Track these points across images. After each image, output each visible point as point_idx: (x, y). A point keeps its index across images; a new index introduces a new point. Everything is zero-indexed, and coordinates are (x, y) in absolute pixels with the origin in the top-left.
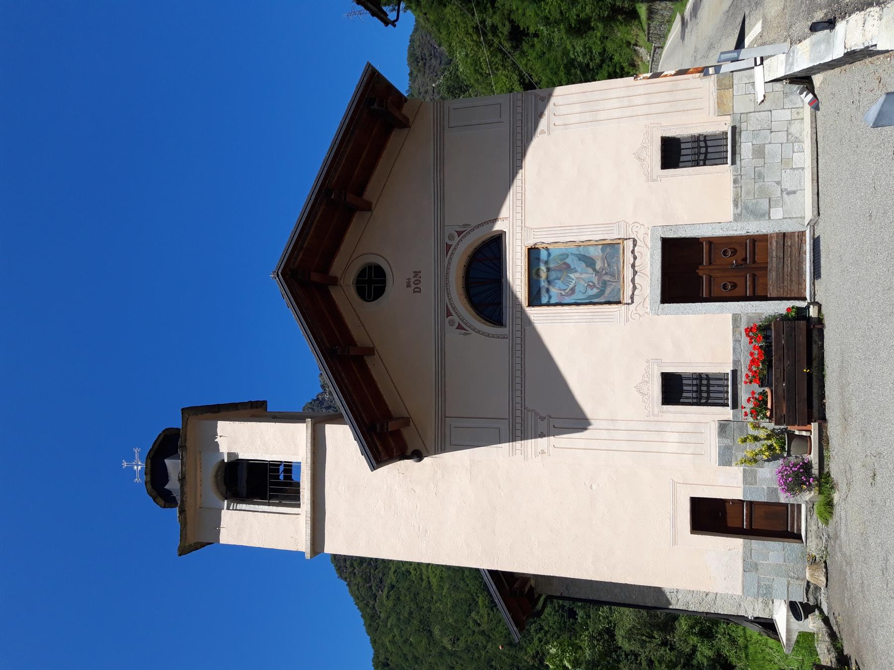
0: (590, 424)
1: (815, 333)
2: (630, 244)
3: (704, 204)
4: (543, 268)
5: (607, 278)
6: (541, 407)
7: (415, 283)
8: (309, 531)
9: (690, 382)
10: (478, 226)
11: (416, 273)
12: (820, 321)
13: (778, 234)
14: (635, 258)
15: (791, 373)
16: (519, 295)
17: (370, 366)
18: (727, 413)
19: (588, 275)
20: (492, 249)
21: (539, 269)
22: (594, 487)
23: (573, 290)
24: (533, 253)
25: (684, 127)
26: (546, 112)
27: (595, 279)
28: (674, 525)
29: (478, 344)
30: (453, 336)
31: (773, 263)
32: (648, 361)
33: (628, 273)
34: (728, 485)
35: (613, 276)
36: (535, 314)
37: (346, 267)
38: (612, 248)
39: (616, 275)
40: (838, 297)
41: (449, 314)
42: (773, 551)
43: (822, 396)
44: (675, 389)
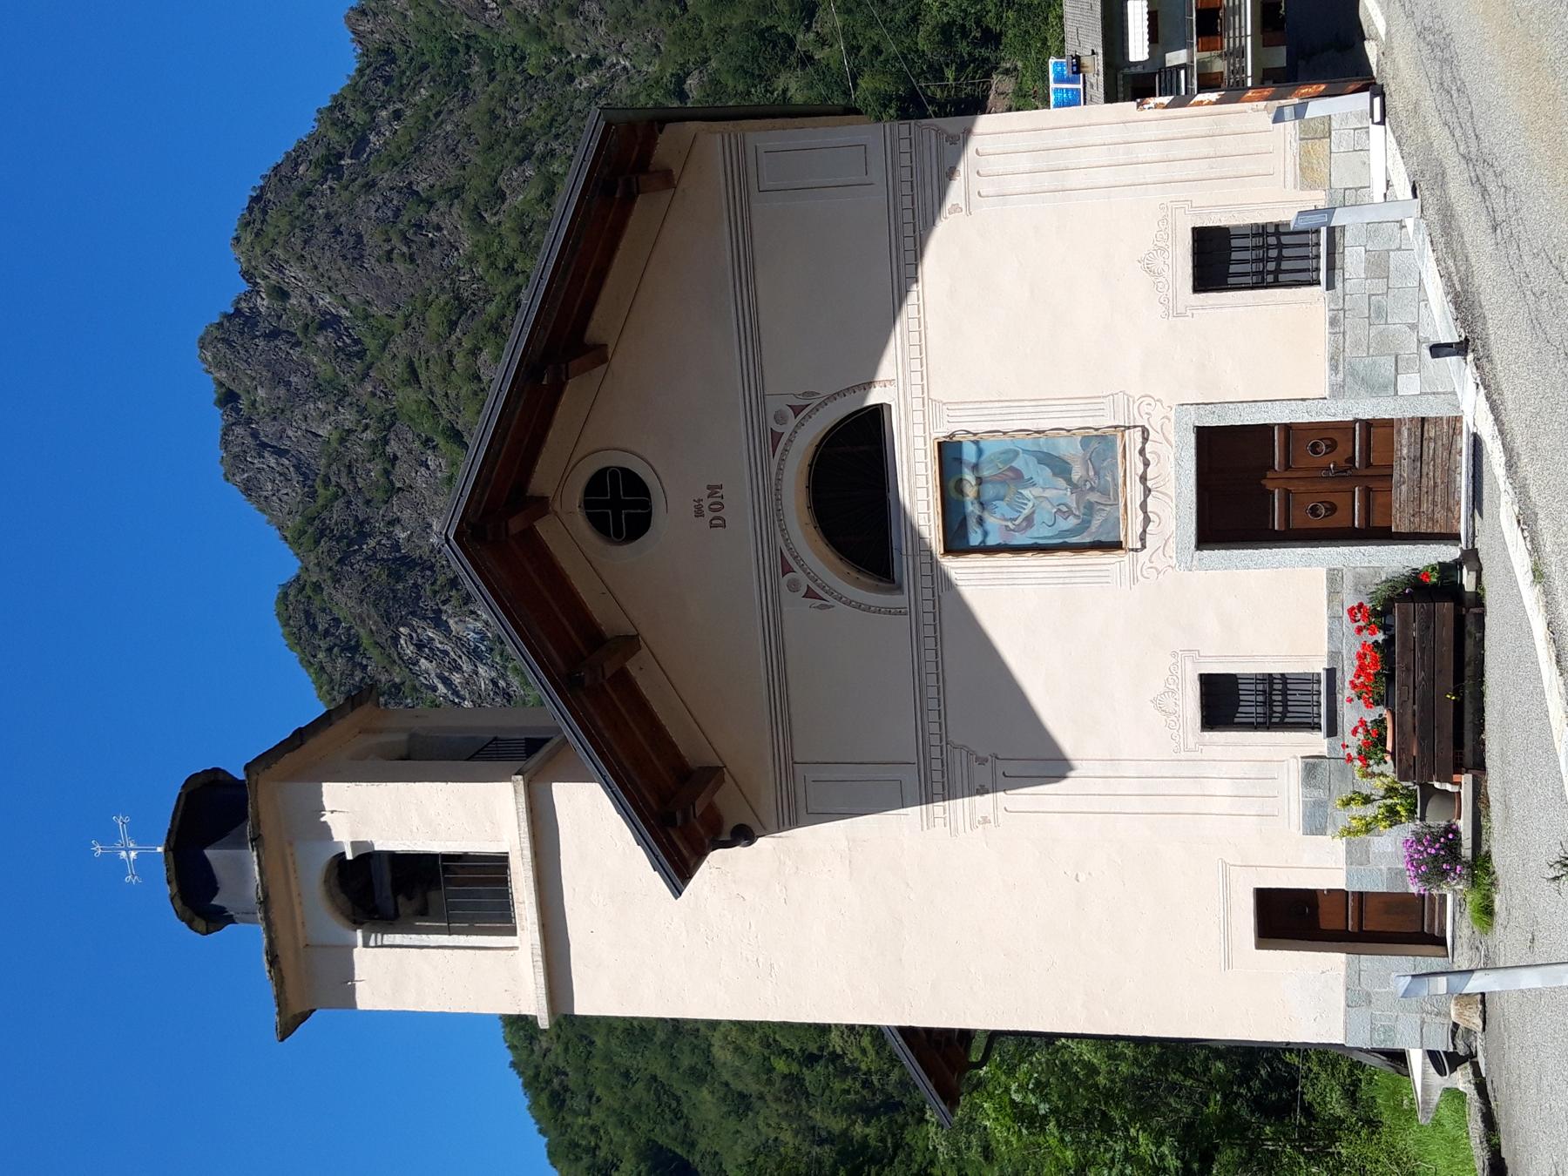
0: (1071, 769)
3: (1275, 361)
4: (969, 477)
5: (1093, 497)
6: (979, 738)
7: (712, 507)
8: (541, 980)
10: (833, 397)
11: (714, 489)
14: (1146, 464)
16: (925, 531)
18: (1316, 742)
19: (1059, 491)
20: (861, 443)
23: (1029, 520)
24: (949, 454)
26: (961, 168)
27: (1072, 500)
28: (1227, 937)
30: (796, 610)
31: (1403, 470)
32: (1174, 654)
33: (1134, 492)
34: (1321, 866)
35: (1105, 493)
36: (959, 569)
38: (1100, 444)
41: (787, 569)
42: (1392, 971)
44: (1223, 702)
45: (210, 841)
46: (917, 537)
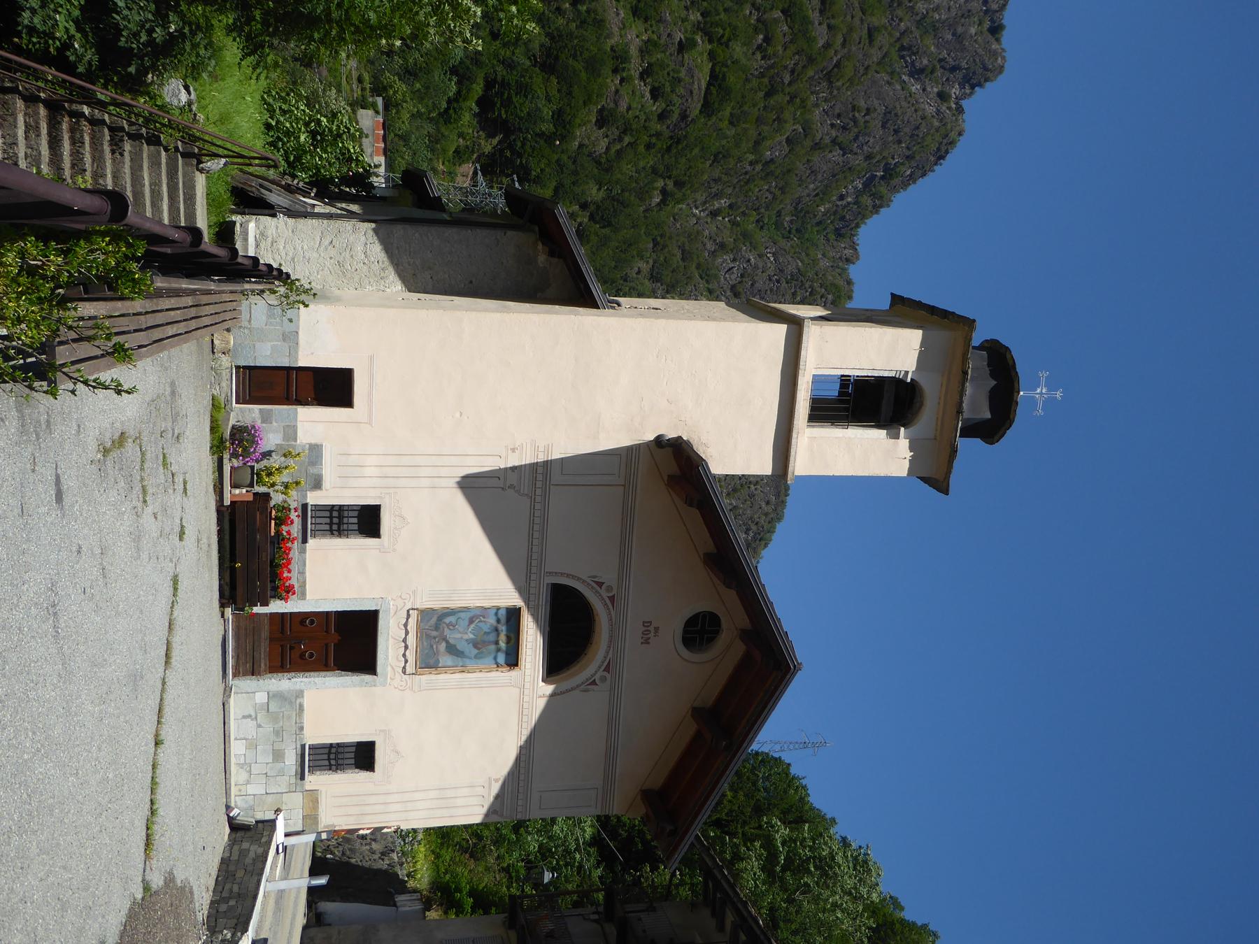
0: (458, 483)
1: (227, 593)
2: (410, 669)
3: (331, 705)
4: (503, 645)
5: (434, 633)
6: (511, 501)
7: (648, 632)
8: (803, 353)
9: (351, 527)
10: (572, 689)
11: (647, 642)
12: (223, 606)
13: (259, 674)
14: (404, 655)
15: (251, 549)
16: (530, 619)
17: (710, 541)
18: (313, 498)
19: (453, 636)
21: (508, 643)
22: (458, 415)
23: (471, 621)
24: (513, 661)
25: (350, 781)
26: (492, 799)
27: (447, 632)
28: (371, 377)
29: (580, 565)
30: (609, 577)
32: (394, 550)
33: (412, 640)
34: (313, 422)
36: (515, 600)
37: (728, 649)
38: (428, 663)
39: (422, 634)
40: (205, 623)
41: (612, 599)
42: (267, 355)
44: (368, 521)
45: (988, 420)
46: (536, 619)
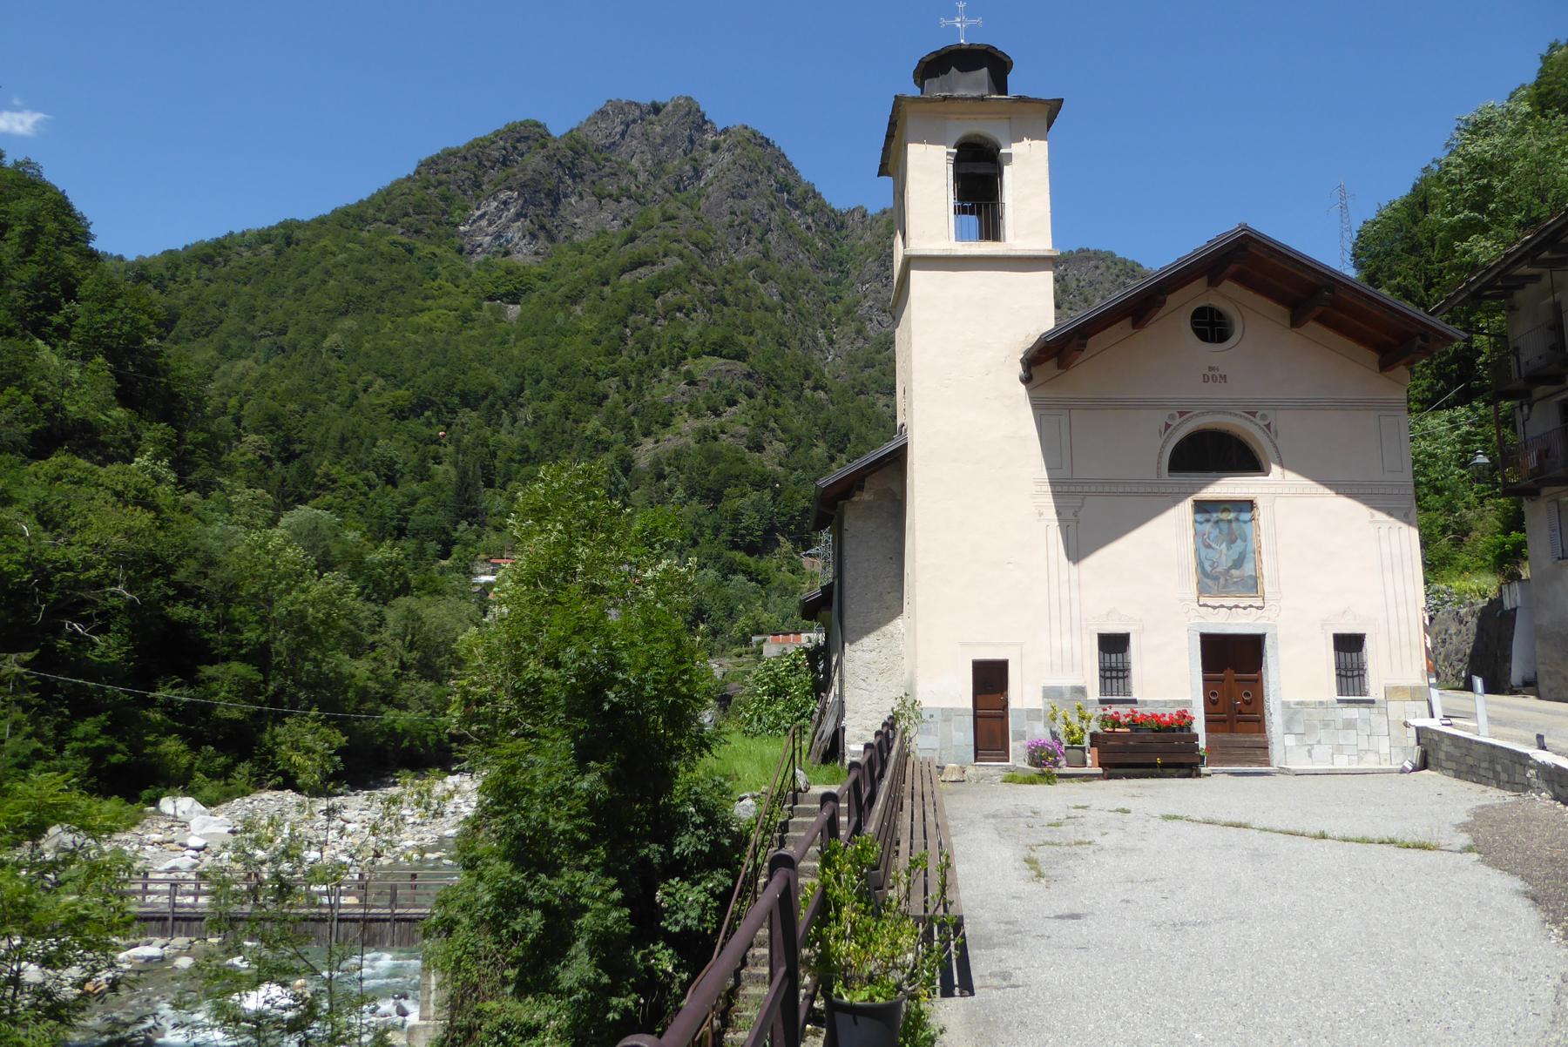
1: (1186, 771)
2: (1259, 603)
3: (1296, 675)
4: (1231, 516)
5: (1222, 580)
6: (1090, 513)
7: (1213, 376)
11: (1224, 378)
12: (1199, 775)
15: (1144, 750)
18: (1094, 693)
19: (1225, 563)
20: (1249, 463)
23: (1209, 546)
24: (1249, 505)
27: (1220, 569)
29: (1150, 445)
30: (1160, 418)
31: (1240, 738)
34: (1022, 695)
35: (1225, 586)
36: (1186, 506)
37: (1228, 298)
38: (1252, 586)
39: (1224, 591)
40: (1216, 791)
41: (1182, 414)
42: (964, 735)
43: (1128, 777)
44: (1114, 645)
46: (1206, 485)
